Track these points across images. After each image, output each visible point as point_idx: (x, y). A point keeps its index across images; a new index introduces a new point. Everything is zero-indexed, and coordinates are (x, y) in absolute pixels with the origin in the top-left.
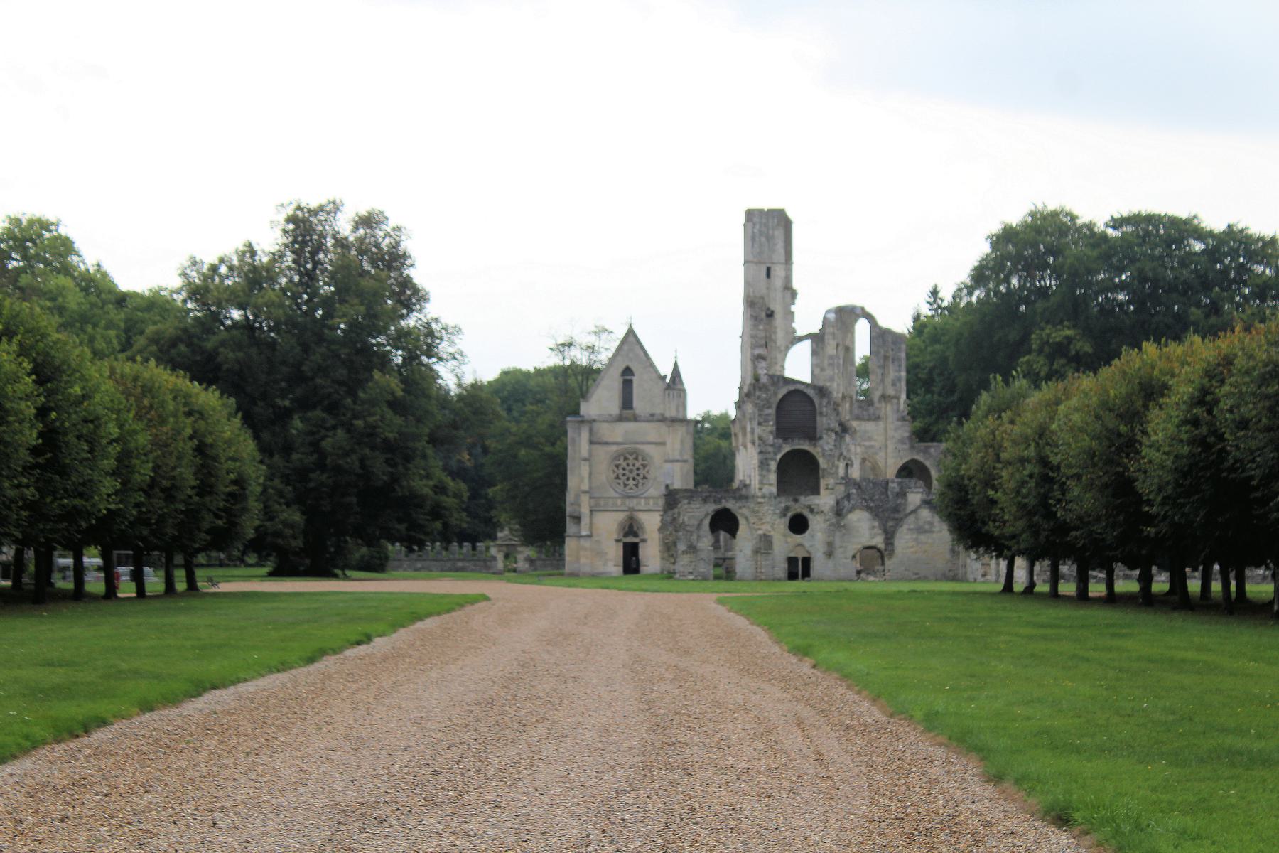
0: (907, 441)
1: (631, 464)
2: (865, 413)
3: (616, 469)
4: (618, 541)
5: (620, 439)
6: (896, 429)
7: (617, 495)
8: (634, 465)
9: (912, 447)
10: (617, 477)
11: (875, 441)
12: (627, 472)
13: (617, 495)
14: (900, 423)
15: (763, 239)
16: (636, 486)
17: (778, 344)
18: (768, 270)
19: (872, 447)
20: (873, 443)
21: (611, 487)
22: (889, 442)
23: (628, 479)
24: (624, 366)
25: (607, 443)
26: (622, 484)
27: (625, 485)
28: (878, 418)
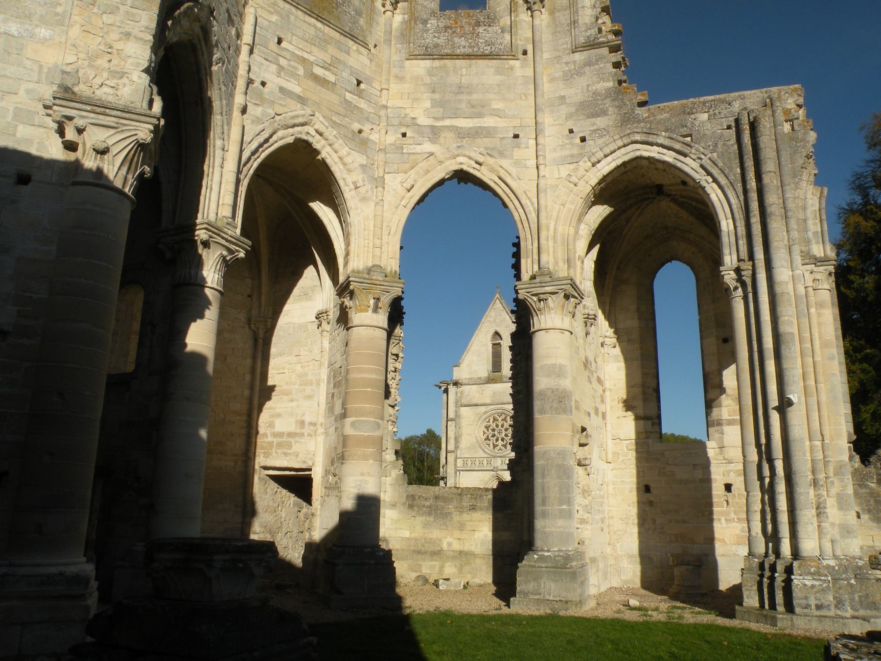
3: (486, 431)
5: (488, 401)
6: (568, 77)
7: (486, 456)
8: (502, 426)
9: (626, 120)
10: (487, 439)
11: (497, 113)
12: (496, 433)
13: (486, 456)
14: (579, 57)
20: (489, 122)
21: (480, 447)
22: (547, 119)
23: (497, 440)
25: (476, 405)
26: (491, 445)
27: (495, 446)
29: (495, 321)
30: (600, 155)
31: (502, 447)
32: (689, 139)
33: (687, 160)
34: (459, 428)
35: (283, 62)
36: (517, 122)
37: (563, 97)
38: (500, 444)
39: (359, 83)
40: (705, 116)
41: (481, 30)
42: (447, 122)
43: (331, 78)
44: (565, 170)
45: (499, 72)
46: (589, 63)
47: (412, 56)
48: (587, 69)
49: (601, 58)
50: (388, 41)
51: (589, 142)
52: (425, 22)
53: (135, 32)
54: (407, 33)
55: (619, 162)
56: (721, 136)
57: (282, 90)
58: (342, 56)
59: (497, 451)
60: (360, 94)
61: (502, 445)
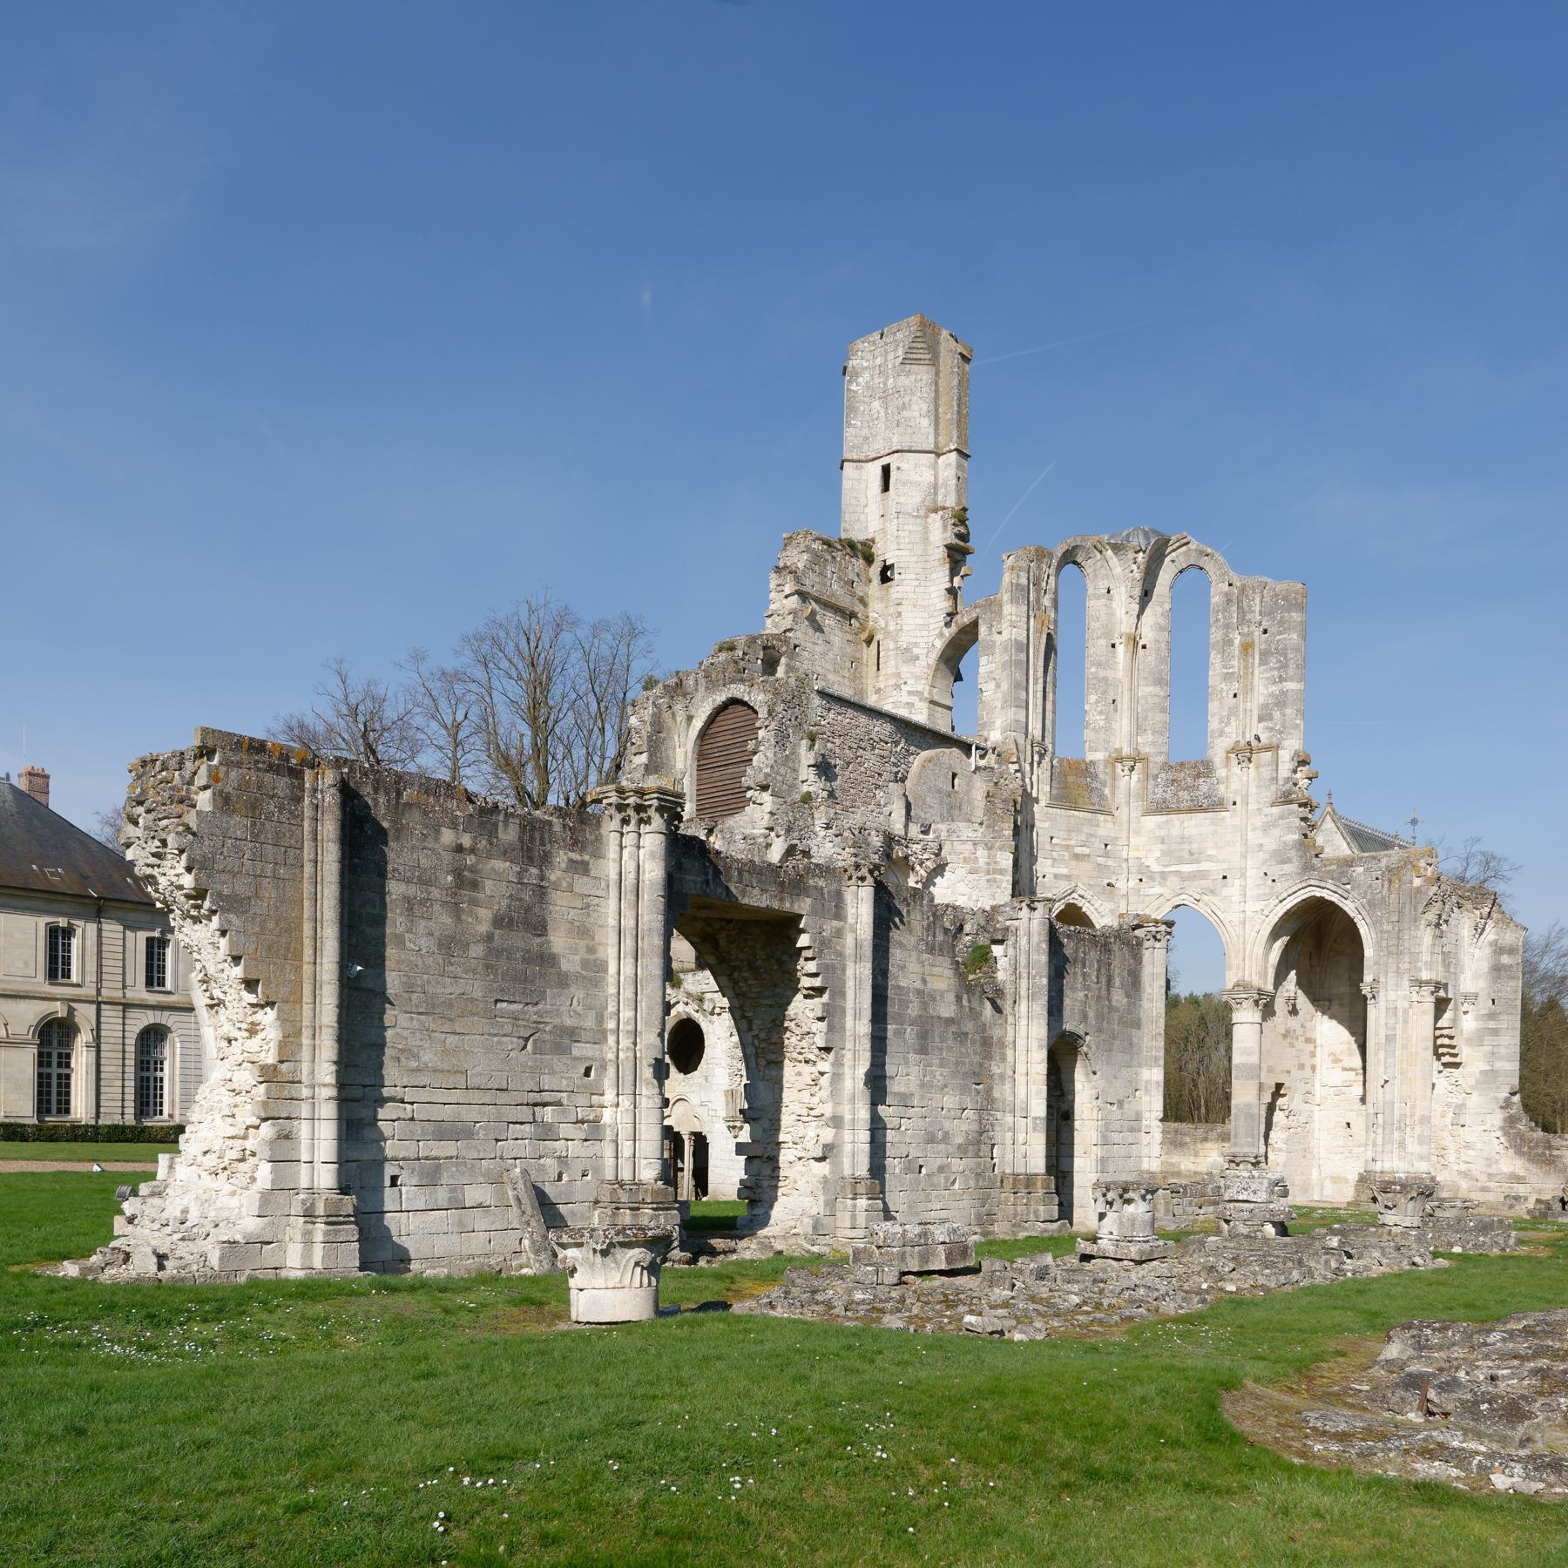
0: (1293, 853)
2: (1184, 795)
6: (1266, 828)
14: (1276, 810)
28: (1215, 805)
30: (1285, 895)
32: (1348, 887)
33: (1347, 902)
36: (1225, 866)
37: (1261, 845)
40: (1361, 869)
41: (1201, 780)
44: (1259, 906)
46: (1281, 817)
47: (1147, 813)
48: (1280, 822)
49: (1291, 813)
51: (1277, 884)
55: (1300, 899)
56: (1370, 886)
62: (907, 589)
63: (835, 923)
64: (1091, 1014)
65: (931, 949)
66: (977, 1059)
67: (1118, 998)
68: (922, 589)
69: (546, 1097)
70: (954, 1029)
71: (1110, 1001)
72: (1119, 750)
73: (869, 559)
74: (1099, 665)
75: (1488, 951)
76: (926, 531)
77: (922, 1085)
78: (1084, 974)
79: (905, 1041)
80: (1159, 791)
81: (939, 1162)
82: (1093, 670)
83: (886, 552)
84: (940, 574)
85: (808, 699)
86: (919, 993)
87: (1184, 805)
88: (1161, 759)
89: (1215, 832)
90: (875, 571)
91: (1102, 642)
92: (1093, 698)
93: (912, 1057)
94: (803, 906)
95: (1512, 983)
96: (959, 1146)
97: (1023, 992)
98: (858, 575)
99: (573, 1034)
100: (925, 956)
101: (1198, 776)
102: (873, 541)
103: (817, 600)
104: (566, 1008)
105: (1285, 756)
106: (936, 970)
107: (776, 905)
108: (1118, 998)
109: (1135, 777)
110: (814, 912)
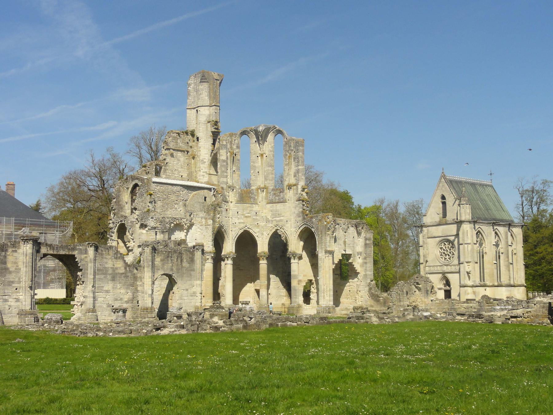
0: (301, 214)
1: (447, 246)
2: (277, 198)
4: (440, 289)
5: (440, 235)
10: (441, 255)
15: (195, 93)
16: (450, 259)
17: (201, 158)
18: (197, 110)
19: (281, 220)
20: (282, 218)
24: (441, 194)
26: (443, 258)
27: (445, 259)
28: (284, 201)
29: (442, 189)
30: (300, 226)
31: (448, 259)
34: (427, 250)
35: (239, 217)
38: (447, 258)
39: (256, 213)
40: (314, 219)
42: (274, 219)
43: (249, 215)
45: (284, 206)
46: (299, 204)
47: (268, 203)
50: (262, 201)
52: (271, 192)
53: (210, 241)
54: (266, 199)
57: (239, 223)
58: (251, 209)
59: (446, 262)
60: (257, 216)
61: (449, 258)
62: (202, 143)
63: (85, 255)
64: (174, 269)
65: (116, 258)
66: (132, 281)
67: (185, 264)
68: (206, 143)
69: (6, 294)
70: (124, 275)
71: (182, 265)
72: (259, 186)
73: (193, 135)
74: (253, 162)
75: (364, 239)
76: (207, 127)
77: (113, 288)
78: (172, 260)
79: (108, 279)
80: (271, 197)
81: (119, 305)
82: (252, 164)
83: (198, 134)
84: (210, 139)
85: (150, 184)
86: (112, 268)
87: (277, 201)
88: (272, 188)
89: (284, 209)
90: (195, 138)
91: (254, 156)
92: (252, 172)
93: (110, 282)
94: (76, 253)
95: (370, 249)
96: (126, 301)
97: (146, 266)
98: (189, 140)
99: (13, 282)
100: (114, 260)
101: (280, 192)
102: (194, 130)
103: (174, 150)
104: (11, 277)
105: (300, 187)
106: (118, 263)
107: (67, 253)
108: (185, 264)
109: (264, 193)
110: (78, 253)
